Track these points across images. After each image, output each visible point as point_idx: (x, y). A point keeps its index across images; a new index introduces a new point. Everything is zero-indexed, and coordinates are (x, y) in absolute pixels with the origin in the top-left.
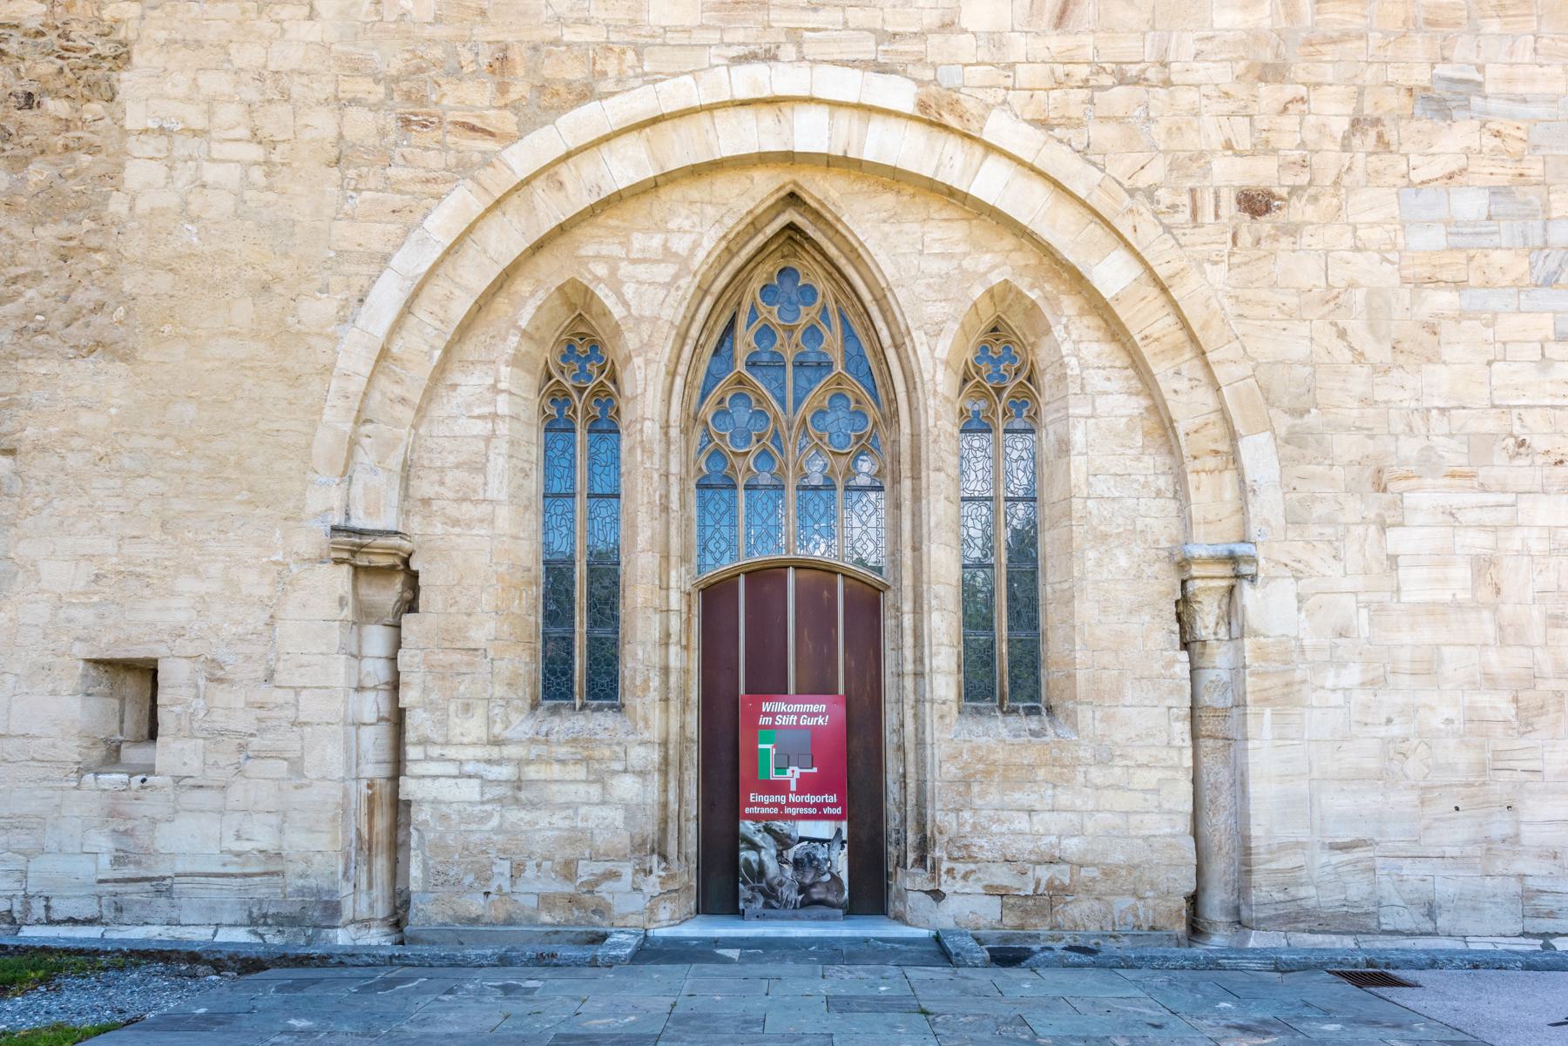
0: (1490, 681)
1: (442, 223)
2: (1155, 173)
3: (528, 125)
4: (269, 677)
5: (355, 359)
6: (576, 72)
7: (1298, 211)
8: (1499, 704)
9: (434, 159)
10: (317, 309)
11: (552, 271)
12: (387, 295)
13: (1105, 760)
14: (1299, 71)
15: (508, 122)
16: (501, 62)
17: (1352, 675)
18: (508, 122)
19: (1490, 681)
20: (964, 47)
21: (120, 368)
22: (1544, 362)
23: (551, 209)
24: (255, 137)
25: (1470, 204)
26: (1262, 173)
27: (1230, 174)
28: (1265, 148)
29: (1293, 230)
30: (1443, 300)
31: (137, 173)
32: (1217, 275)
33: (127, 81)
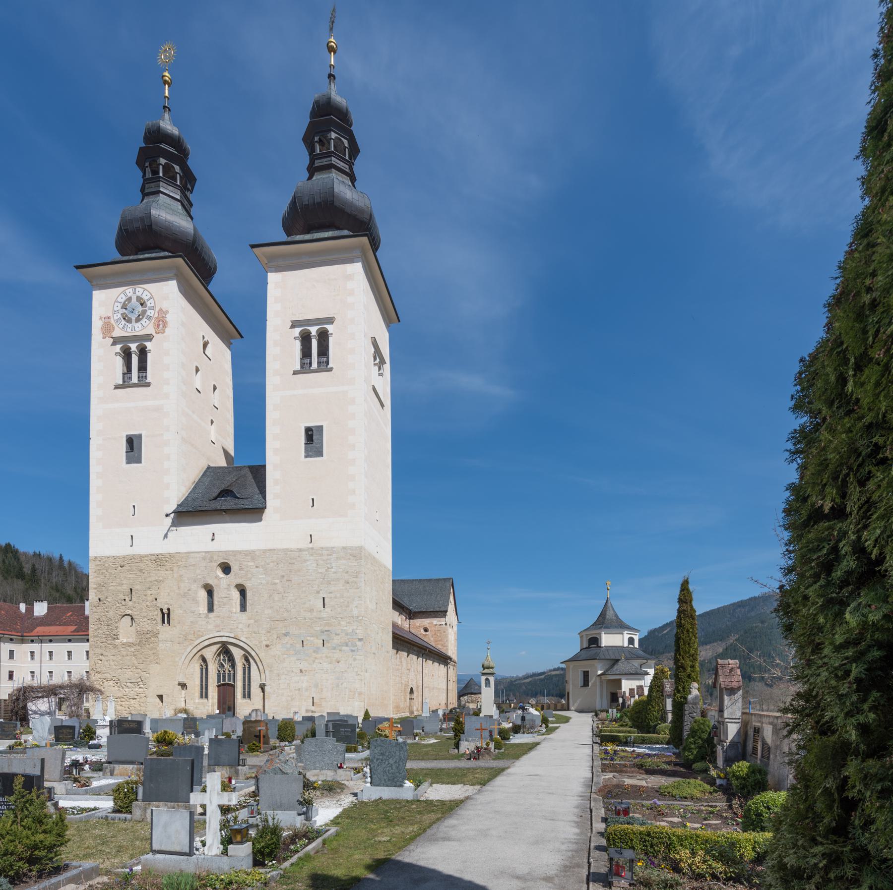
0: (289, 696)
1: (188, 650)
2: (257, 643)
3: (197, 639)
4: (173, 696)
5: (180, 664)
6: (201, 634)
7: (271, 647)
8: (289, 698)
9: (188, 643)
10: (177, 659)
11: (200, 654)
12: (183, 657)
13: (253, 704)
14: (272, 632)
15: (195, 639)
16: (194, 633)
17: (275, 695)
18: (195, 639)
19: (289, 696)
20: (239, 630)
21: (159, 665)
22: (295, 663)
23: (199, 647)
24: (171, 641)
25: (288, 646)
26: (268, 643)
27: (265, 643)
28: (268, 640)
29: (270, 649)
30: (286, 656)
31: (160, 645)
32: (263, 654)
33: (160, 636)
